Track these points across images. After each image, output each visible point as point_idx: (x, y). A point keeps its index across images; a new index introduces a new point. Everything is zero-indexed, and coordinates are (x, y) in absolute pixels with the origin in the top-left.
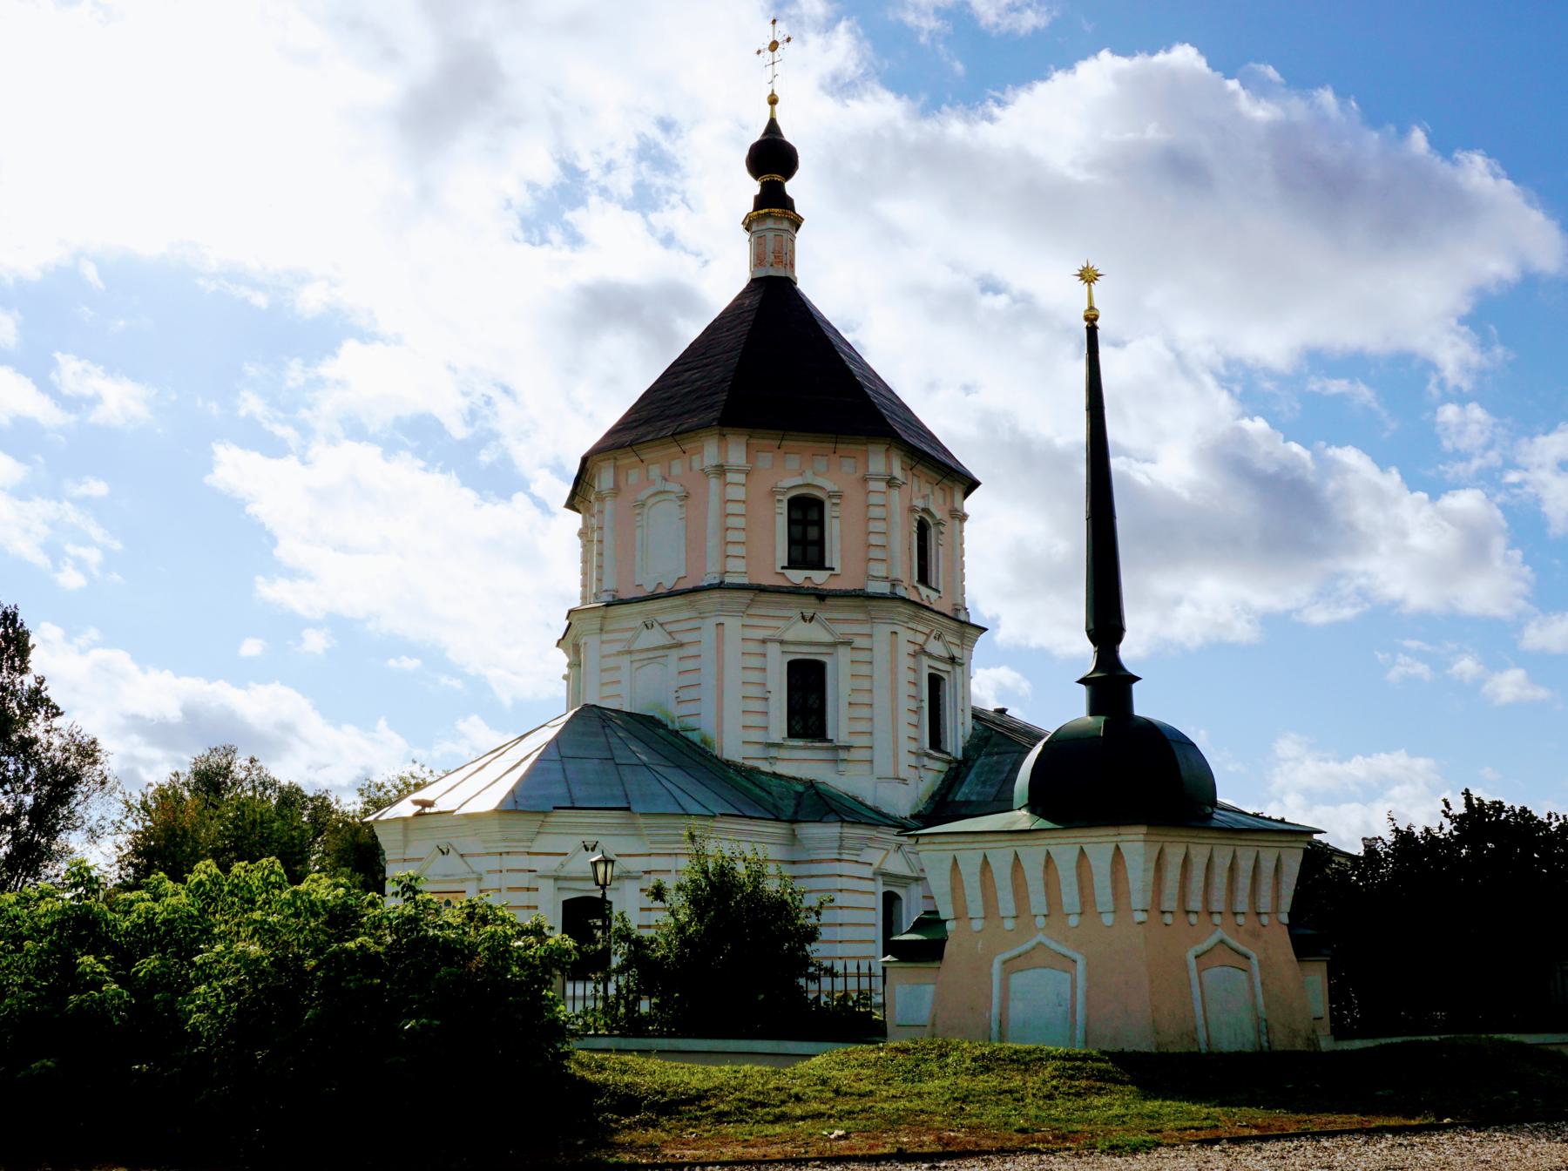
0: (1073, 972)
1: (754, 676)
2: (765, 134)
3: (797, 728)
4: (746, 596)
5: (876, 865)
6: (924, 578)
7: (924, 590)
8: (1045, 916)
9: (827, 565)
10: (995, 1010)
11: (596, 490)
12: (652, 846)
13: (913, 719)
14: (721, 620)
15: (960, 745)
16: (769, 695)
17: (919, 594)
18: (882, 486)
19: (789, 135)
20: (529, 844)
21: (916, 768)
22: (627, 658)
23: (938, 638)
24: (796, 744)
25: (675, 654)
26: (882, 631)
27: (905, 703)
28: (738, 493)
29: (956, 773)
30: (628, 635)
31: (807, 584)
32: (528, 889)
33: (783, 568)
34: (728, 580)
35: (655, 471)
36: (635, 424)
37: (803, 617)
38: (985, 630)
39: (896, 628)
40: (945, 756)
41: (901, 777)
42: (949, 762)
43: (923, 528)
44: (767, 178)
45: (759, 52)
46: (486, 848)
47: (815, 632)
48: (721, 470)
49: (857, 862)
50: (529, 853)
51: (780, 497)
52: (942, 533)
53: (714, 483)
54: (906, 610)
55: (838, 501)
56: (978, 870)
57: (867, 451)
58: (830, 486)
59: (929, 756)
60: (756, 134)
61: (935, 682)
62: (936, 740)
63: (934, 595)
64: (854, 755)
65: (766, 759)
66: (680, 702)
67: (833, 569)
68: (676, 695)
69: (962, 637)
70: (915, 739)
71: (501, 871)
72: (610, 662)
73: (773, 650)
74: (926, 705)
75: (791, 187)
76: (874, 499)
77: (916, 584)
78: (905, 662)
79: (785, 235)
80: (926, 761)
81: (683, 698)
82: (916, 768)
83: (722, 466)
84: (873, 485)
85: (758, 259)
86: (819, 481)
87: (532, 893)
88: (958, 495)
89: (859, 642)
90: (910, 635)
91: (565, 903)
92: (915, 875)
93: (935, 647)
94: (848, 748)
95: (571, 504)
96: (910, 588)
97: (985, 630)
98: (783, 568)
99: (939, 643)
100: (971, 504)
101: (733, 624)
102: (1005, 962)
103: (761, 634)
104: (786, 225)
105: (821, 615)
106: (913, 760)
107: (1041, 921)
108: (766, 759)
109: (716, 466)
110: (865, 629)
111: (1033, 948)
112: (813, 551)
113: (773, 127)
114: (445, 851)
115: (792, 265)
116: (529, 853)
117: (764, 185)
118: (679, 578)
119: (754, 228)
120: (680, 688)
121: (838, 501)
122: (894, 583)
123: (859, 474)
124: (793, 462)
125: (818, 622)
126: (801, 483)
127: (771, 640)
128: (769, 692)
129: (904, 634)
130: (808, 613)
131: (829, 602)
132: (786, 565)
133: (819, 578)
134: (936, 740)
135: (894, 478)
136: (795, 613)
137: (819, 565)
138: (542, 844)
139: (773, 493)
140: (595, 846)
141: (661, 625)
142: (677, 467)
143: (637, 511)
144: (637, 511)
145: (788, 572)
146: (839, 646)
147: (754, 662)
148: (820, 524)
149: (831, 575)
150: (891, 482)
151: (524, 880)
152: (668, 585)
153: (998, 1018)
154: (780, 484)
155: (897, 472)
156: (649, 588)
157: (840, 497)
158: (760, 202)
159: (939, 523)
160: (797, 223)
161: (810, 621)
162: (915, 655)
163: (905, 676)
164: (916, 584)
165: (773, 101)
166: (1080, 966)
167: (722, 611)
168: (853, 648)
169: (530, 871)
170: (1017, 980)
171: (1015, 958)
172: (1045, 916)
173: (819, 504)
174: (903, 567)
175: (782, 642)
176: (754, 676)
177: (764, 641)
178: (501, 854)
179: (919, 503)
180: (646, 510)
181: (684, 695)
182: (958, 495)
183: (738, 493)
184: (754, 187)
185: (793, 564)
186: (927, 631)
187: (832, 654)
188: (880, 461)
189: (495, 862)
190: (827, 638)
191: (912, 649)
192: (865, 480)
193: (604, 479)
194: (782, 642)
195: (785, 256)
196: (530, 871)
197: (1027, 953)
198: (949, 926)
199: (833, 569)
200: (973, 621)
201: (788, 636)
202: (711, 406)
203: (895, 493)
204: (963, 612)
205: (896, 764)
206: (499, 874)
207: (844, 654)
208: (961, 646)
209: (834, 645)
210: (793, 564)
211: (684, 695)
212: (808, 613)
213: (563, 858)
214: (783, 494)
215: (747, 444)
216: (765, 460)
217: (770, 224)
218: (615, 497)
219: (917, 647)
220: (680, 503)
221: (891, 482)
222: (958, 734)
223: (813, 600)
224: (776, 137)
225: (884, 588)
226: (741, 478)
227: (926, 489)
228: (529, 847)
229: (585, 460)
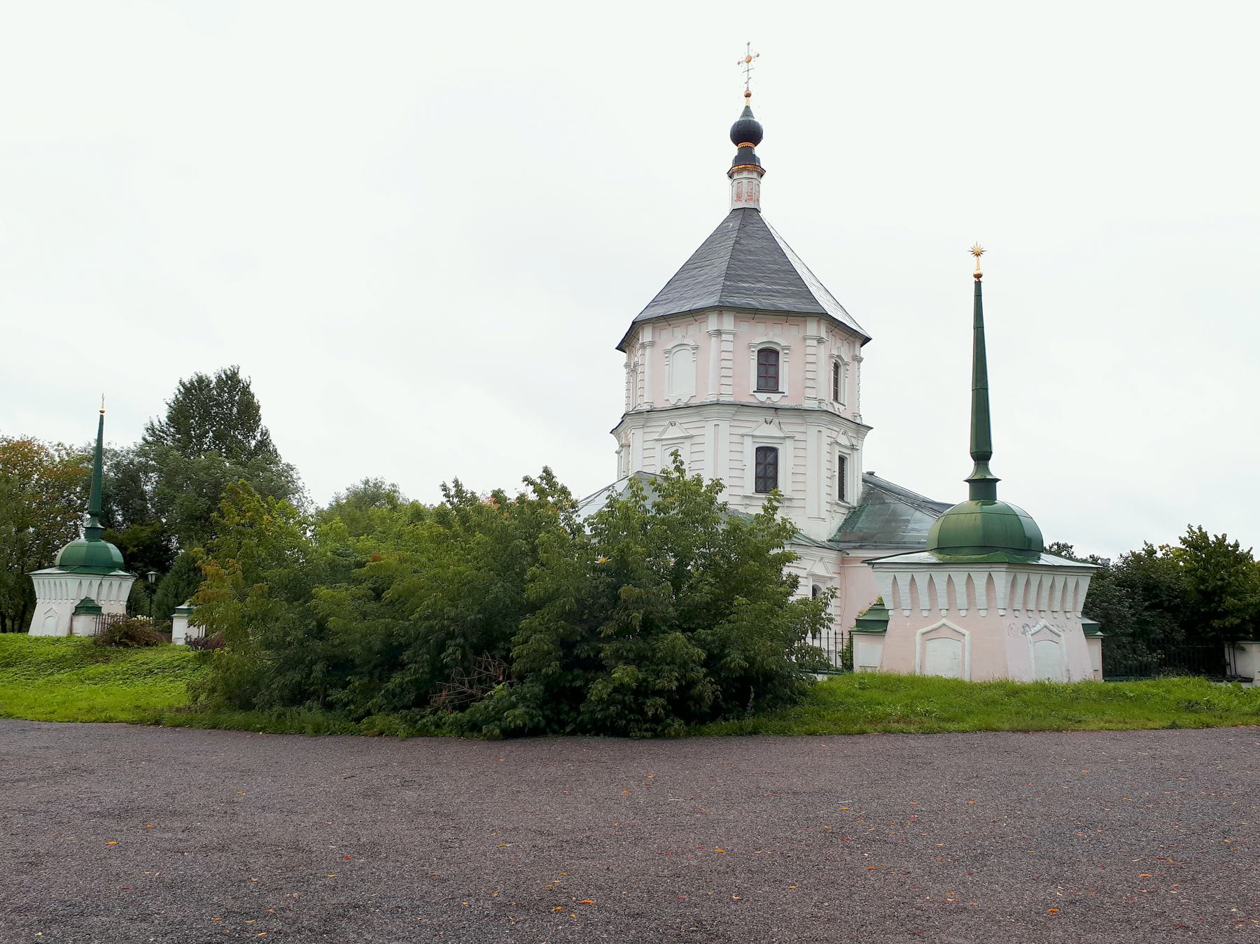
0: (963, 641)
2: (743, 116)
3: (761, 486)
4: (732, 410)
5: (808, 570)
6: (836, 398)
8: (947, 610)
9: (780, 390)
10: (918, 660)
11: (640, 341)
13: (828, 482)
15: (856, 498)
17: (834, 407)
18: (815, 343)
19: (758, 117)
21: (830, 511)
22: (658, 446)
23: (844, 433)
24: (760, 496)
26: (812, 431)
27: (825, 473)
28: (730, 347)
29: (854, 515)
31: (769, 402)
33: (754, 392)
34: (723, 399)
35: (677, 330)
36: (666, 302)
37: (766, 421)
38: (872, 428)
39: (820, 428)
40: (847, 505)
41: (822, 517)
42: (849, 508)
43: (836, 367)
45: (739, 63)
48: (719, 333)
49: (798, 567)
51: (754, 349)
52: (848, 370)
53: (714, 339)
54: (826, 417)
55: (787, 352)
56: (908, 582)
57: (806, 321)
59: (837, 504)
60: (736, 117)
61: (842, 460)
62: (842, 496)
63: (842, 408)
64: (795, 503)
65: (743, 505)
67: (784, 393)
69: (858, 432)
70: (830, 494)
72: (648, 445)
73: (748, 441)
74: (837, 474)
75: (758, 150)
76: (809, 350)
77: (832, 401)
78: (826, 448)
79: (754, 182)
80: (836, 508)
82: (830, 511)
83: (720, 330)
84: (809, 342)
85: (739, 197)
88: (858, 345)
89: (798, 437)
90: (829, 432)
92: (830, 575)
93: (843, 440)
94: (790, 499)
95: (620, 348)
96: (829, 404)
97: (872, 428)
98: (754, 392)
99: (845, 437)
100: (865, 351)
101: (724, 426)
102: (923, 634)
104: (755, 175)
105: (776, 421)
106: (828, 507)
107: (944, 612)
108: (743, 505)
110: (802, 429)
111: (940, 627)
112: (771, 382)
113: (747, 111)
115: (758, 200)
119: (736, 176)
121: (787, 352)
122: (820, 401)
124: (761, 328)
125: (774, 424)
126: (766, 340)
127: (746, 435)
129: (825, 432)
130: (769, 420)
131: (780, 412)
133: (775, 398)
134: (842, 496)
135: (823, 338)
137: (776, 391)
141: (680, 424)
143: (666, 355)
144: (666, 355)
145: (755, 394)
148: (776, 365)
150: (820, 341)
153: (919, 664)
154: (754, 341)
155: (823, 335)
157: (788, 349)
158: (737, 161)
159: (846, 364)
160: (761, 173)
163: (825, 457)
164: (832, 401)
165: (748, 95)
166: (967, 638)
170: (932, 645)
171: (932, 631)
172: (947, 610)
174: (826, 392)
175: (753, 436)
177: (742, 436)
179: (835, 352)
182: (858, 345)
183: (730, 347)
184: (734, 150)
185: (759, 390)
186: (838, 430)
188: (813, 329)
190: (782, 435)
193: (646, 336)
195: (754, 196)
197: (936, 629)
198: (890, 613)
199: (784, 393)
200: (864, 423)
201: (755, 433)
202: (713, 293)
203: (822, 346)
204: (858, 417)
205: (819, 509)
207: (789, 443)
208: (856, 438)
209: (784, 438)
210: (759, 390)
212: (769, 420)
214: (754, 347)
215: (735, 317)
217: (745, 174)
219: (833, 439)
221: (820, 341)
222: (855, 492)
224: (751, 119)
225: (813, 405)
226: (731, 338)
227: (839, 343)
229: (634, 323)
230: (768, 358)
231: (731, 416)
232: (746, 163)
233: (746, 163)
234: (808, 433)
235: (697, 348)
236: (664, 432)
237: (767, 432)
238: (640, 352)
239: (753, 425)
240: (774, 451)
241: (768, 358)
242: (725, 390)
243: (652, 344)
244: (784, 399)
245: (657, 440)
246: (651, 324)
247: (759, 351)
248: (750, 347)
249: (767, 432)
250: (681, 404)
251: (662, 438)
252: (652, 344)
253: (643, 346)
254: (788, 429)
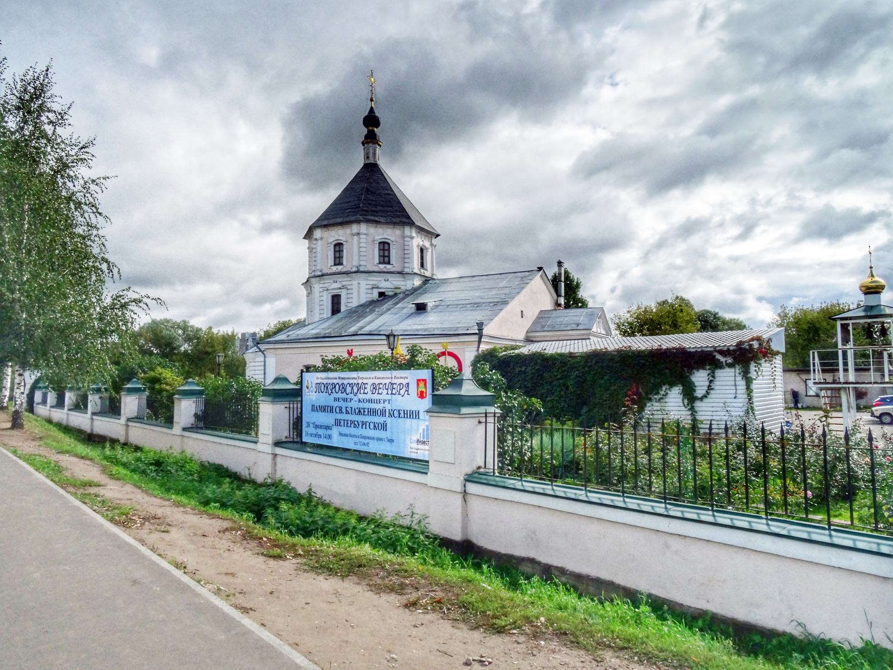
7: (382, 266)
19: (377, 113)
26: (355, 283)
44: (370, 128)
63: (388, 266)
86: (340, 238)
89: (349, 287)
113: (372, 110)
117: (368, 131)
132: (333, 264)
133: (340, 268)
136: (331, 281)
137: (341, 264)
158: (366, 137)
162: (373, 288)
173: (342, 244)
185: (335, 265)
191: (370, 287)
230: (338, 247)
232: (371, 139)
233: (371, 139)
237: (334, 286)
240: (340, 295)
241: (338, 247)
247: (335, 245)
249: (334, 286)
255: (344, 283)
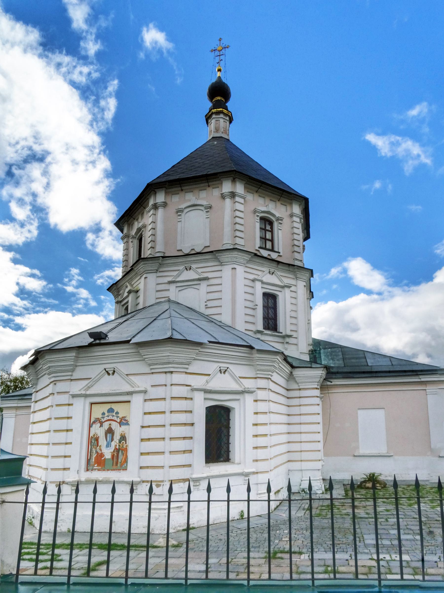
1: (249, 297)
9: (276, 250)
12: (258, 372)
14: (235, 266)
16: (257, 307)
20: (187, 366)
22: (172, 287)
25: (204, 284)
30: (175, 273)
31: (269, 257)
32: (186, 398)
33: (260, 248)
46: (151, 369)
47: (273, 279)
48: (233, 195)
50: (186, 373)
53: (228, 201)
58: (277, 215)
66: (207, 307)
67: (279, 253)
68: (206, 304)
71: (166, 385)
73: (258, 285)
81: (209, 306)
86: (273, 211)
87: (188, 401)
91: (206, 408)
101: (240, 270)
103: (252, 277)
109: (230, 192)
114: (111, 372)
116: (186, 373)
118: (205, 247)
120: (207, 300)
123: (289, 213)
124: (261, 201)
125: (275, 275)
128: (257, 305)
130: (272, 270)
136: (266, 270)
137: (272, 250)
138: (195, 367)
139: (255, 211)
140: (226, 370)
142: (203, 194)
146: (286, 288)
147: (250, 290)
149: (279, 256)
151: (183, 391)
152: (198, 250)
156: (187, 251)
157: (282, 220)
161: (272, 274)
167: (236, 262)
168: (291, 291)
169: (187, 386)
175: (263, 283)
176: (249, 297)
177: (253, 281)
178: (166, 372)
180: (183, 214)
181: (210, 304)
183: (241, 207)
187: (281, 291)
189: (161, 379)
192: (292, 216)
194: (263, 283)
196: (187, 386)
201: (265, 280)
206: (164, 387)
211: (210, 304)
213: (206, 378)
214: (259, 212)
216: (250, 197)
218: (164, 207)
220: (206, 210)
223: (274, 264)
226: (242, 201)
228: (187, 368)
231: (245, 262)
234: (298, 286)
235: (210, 207)
236: (179, 275)
238: (152, 212)
239: (259, 273)
242: (238, 241)
243: (165, 205)
244: (279, 257)
245: (170, 282)
246: (164, 189)
248: (255, 211)
250: (193, 252)
251: (177, 280)
252: (165, 205)
253: (155, 207)
254: (287, 281)
255: (287, 281)
